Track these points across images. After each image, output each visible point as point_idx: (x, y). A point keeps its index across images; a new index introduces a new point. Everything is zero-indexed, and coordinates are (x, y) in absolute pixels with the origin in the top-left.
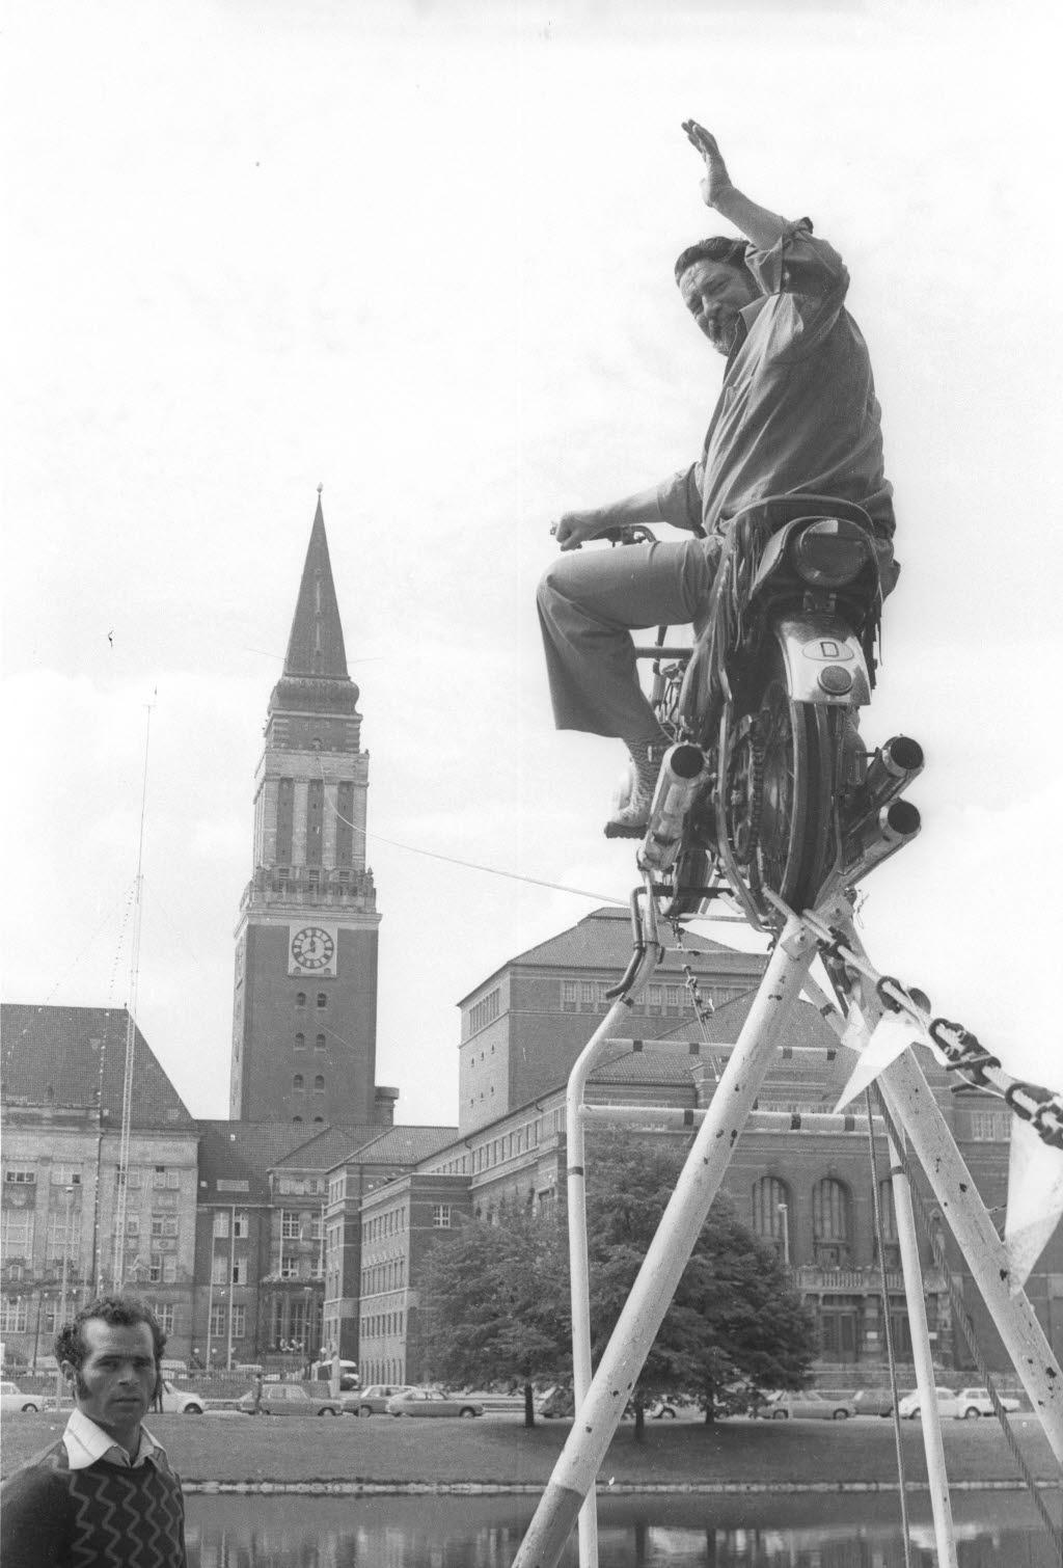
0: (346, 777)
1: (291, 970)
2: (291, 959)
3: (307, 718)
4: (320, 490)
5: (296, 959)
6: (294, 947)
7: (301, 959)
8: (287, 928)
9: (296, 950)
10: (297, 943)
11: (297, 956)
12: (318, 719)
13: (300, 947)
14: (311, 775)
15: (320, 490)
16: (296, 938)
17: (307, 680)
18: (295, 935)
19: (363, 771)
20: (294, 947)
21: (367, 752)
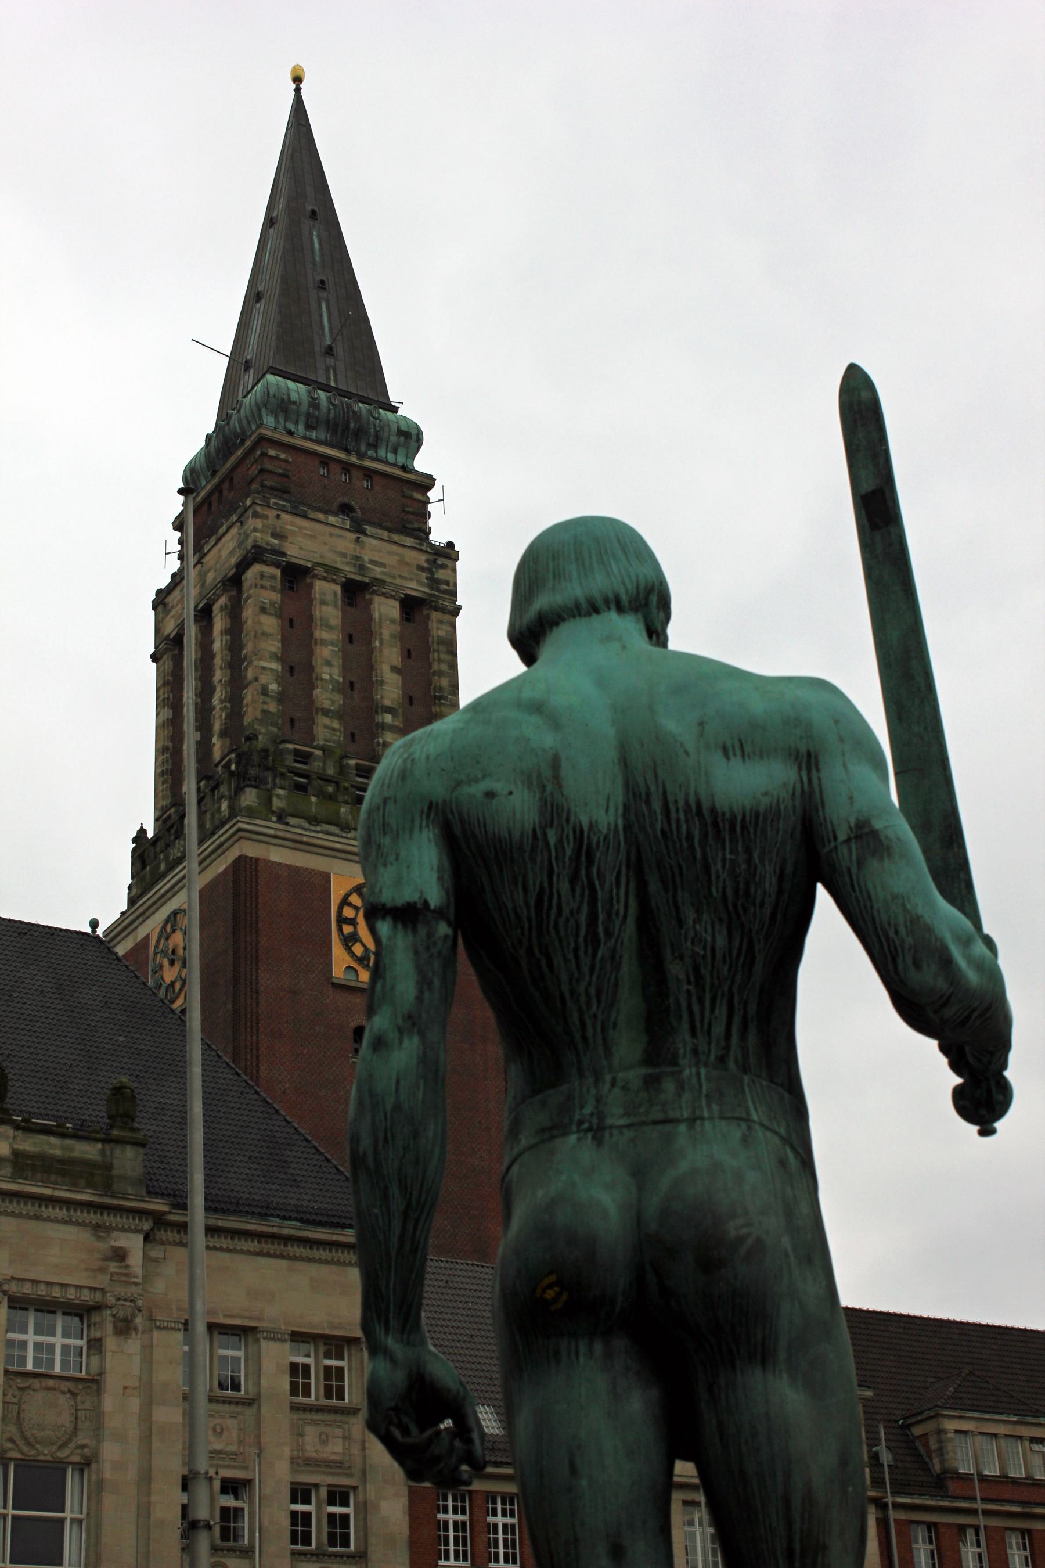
0: (416, 587)
1: (338, 972)
2: (337, 950)
3: (325, 461)
4: (298, 80)
5: (352, 954)
6: (342, 920)
7: (358, 949)
8: (326, 877)
9: (347, 929)
10: (348, 913)
11: (349, 941)
12: (347, 467)
13: (352, 922)
14: (350, 571)
15: (298, 80)
16: (345, 902)
18: (342, 893)
19: (447, 583)
20: (342, 920)
21: (450, 545)
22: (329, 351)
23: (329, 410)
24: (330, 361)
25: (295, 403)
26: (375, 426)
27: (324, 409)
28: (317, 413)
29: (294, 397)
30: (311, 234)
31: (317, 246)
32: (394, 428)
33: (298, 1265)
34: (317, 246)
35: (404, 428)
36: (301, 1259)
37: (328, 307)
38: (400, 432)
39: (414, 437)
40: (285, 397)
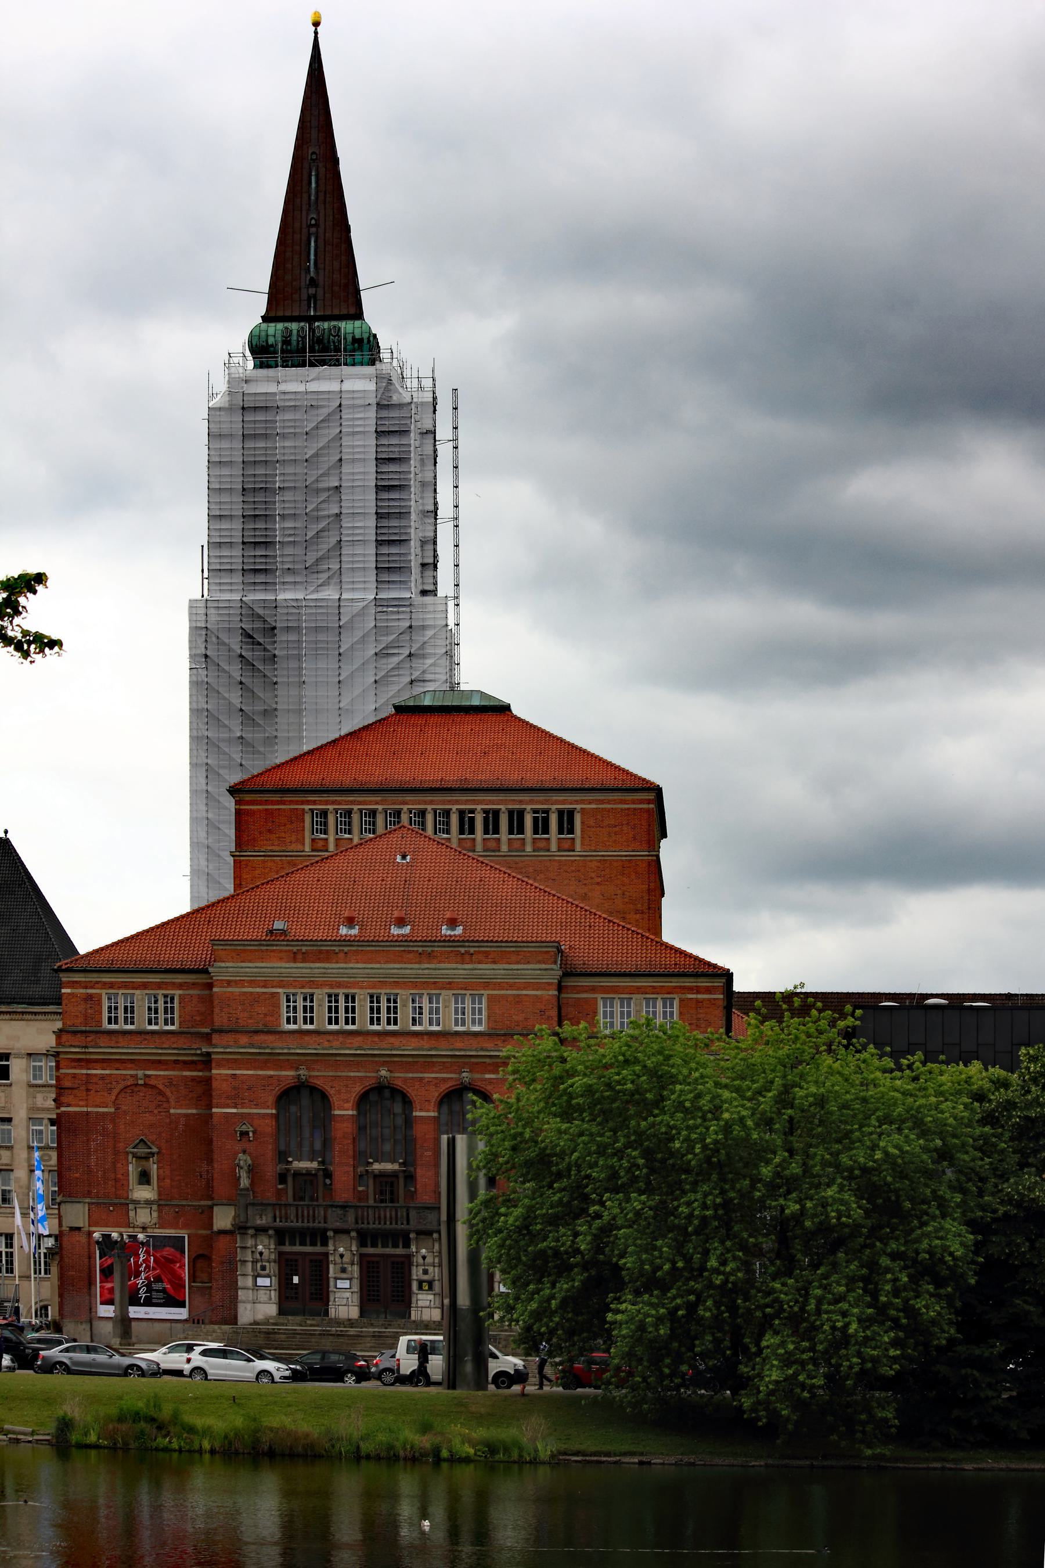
17: (294, 326)
22: (313, 283)
23: (298, 341)
24: (312, 291)
25: (272, 346)
26: (334, 342)
27: (294, 343)
28: (289, 348)
29: (271, 340)
30: (310, 176)
31: (313, 185)
32: (350, 338)
33: (31, 1023)
34: (313, 185)
35: (358, 336)
36: (30, 1020)
37: (316, 242)
38: (355, 340)
39: (365, 341)
40: (264, 344)
